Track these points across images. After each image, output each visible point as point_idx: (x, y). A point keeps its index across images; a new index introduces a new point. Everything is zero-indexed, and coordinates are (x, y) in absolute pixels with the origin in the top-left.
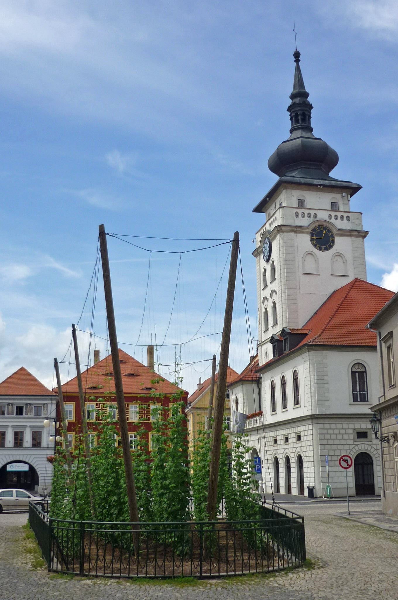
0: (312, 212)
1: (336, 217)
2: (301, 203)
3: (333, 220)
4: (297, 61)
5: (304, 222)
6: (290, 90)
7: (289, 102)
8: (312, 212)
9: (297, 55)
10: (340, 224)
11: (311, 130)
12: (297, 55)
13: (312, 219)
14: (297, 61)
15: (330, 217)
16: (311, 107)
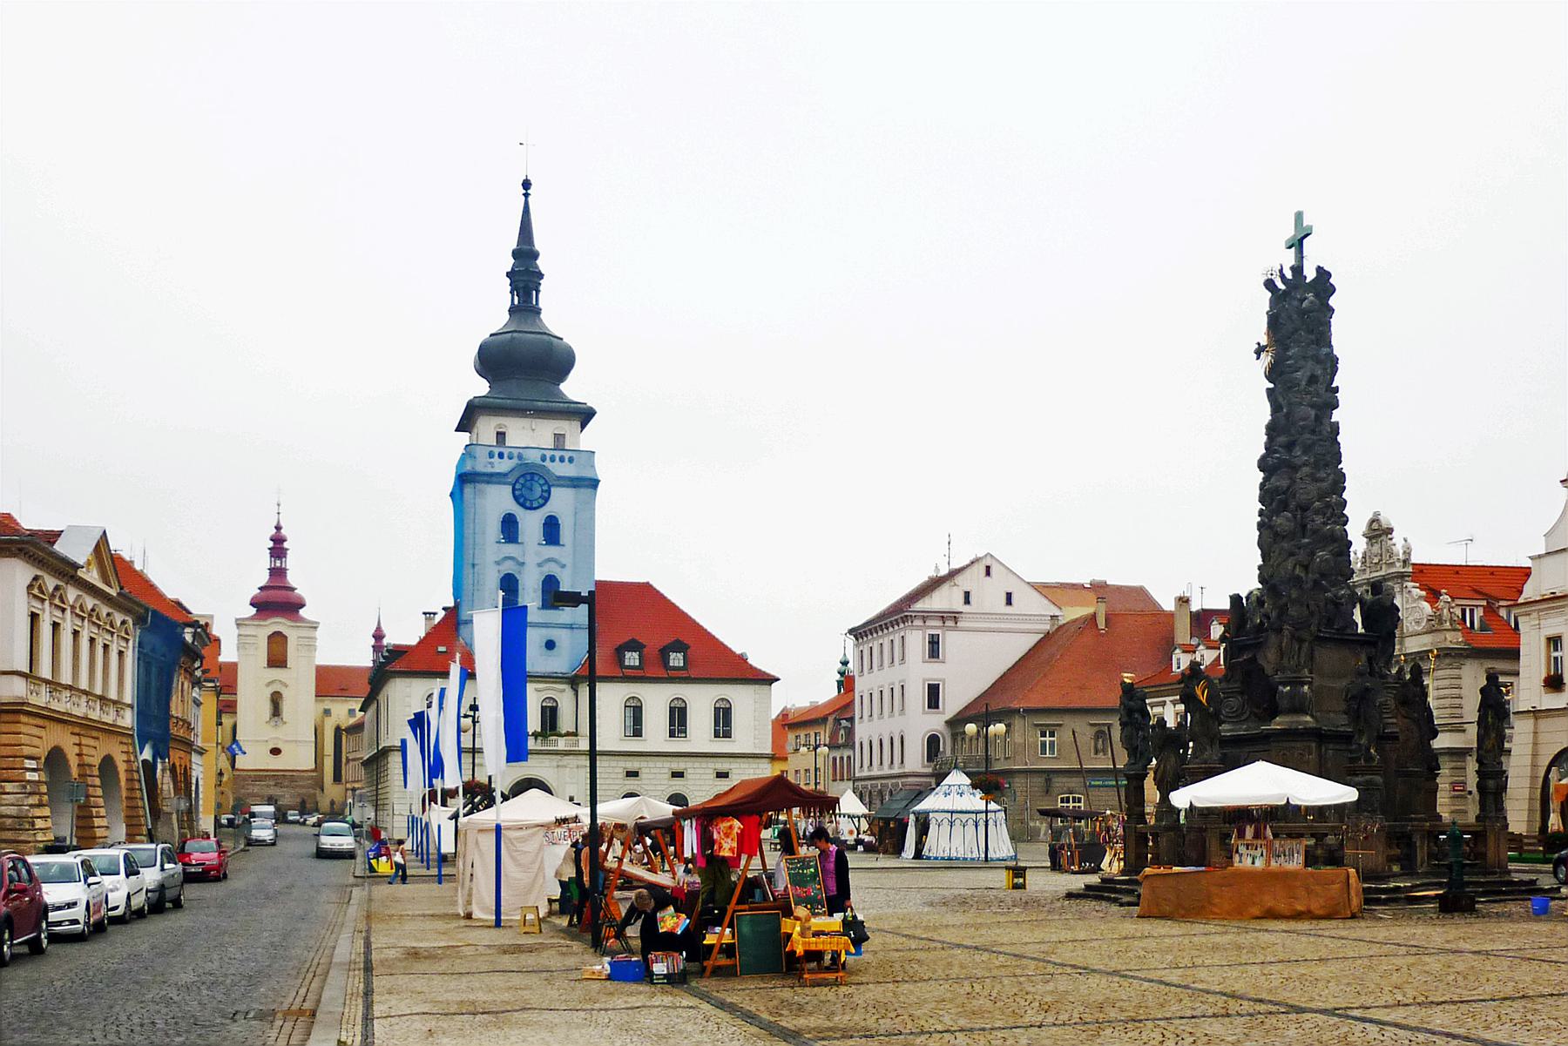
0: (516, 452)
1: (553, 459)
2: (501, 436)
3: (547, 463)
4: (526, 195)
5: (503, 466)
6: (513, 244)
7: (509, 263)
8: (516, 452)
9: (526, 185)
10: (559, 469)
11: (537, 311)
12: (526, 185)
13: (515, 461)
14: (526, 195)
15: (543, 458)
16: (541, 276)
